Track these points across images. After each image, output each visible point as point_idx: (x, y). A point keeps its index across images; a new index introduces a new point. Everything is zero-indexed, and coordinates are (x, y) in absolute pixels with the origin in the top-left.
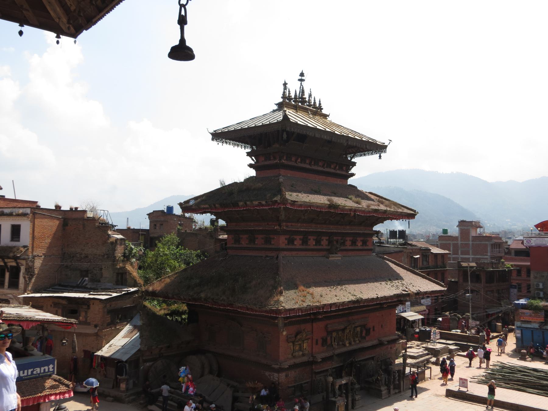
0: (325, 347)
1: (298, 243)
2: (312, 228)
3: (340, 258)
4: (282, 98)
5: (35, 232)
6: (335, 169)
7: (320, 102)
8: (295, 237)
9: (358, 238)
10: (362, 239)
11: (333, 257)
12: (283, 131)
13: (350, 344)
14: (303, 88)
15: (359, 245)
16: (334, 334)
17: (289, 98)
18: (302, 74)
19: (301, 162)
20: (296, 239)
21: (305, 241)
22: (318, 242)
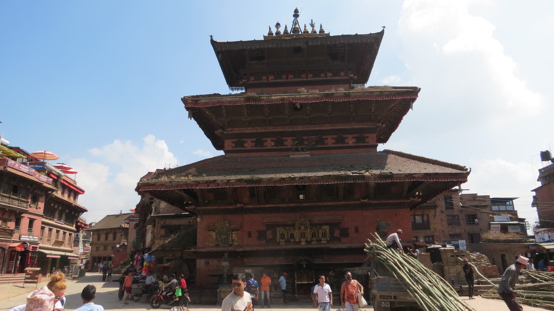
1: (249, 144)
2: (271, 129)
3: (309, 156)
4: (269, 34)
7: (321, 26)
8: (245, 140)
10: (355, 135)
11: (294, 155)
13: (308, 242)
15: (350, 142)
16: (279, 230)
17: (278, 33)
18: (296, 11)
19: (274, 79)
20: (246, 142)
22: (279, 142)
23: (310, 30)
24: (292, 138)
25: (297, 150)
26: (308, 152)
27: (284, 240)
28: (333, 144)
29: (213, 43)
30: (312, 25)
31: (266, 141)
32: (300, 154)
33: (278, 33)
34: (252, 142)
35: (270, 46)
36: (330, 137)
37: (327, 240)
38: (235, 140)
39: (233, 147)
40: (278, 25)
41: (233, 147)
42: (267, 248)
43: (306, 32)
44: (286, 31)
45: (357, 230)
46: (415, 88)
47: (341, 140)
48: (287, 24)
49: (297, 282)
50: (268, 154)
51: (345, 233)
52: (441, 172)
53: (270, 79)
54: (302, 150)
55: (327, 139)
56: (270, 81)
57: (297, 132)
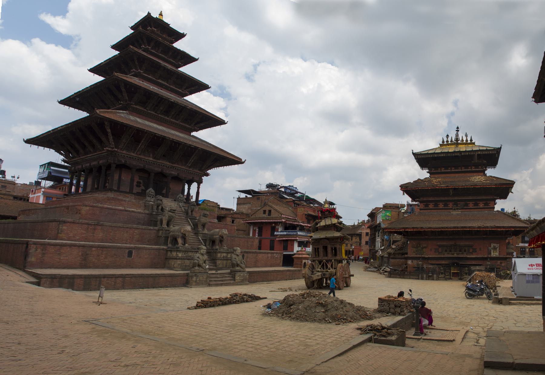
17: (447, 141)
18: (458, 128)
21: (436, 205)
22: (446, 205)
23: (465, 139)
25: (455, 210)
29: (414, 154)
30: (466, 136)
33: (447, 141)
36: (471, 203)
40: (448, 136)
43: (462, 140)
44: (451, 141)
47: (476, 204)
49: (452, 272)
50: (440, 211)
51: (475, 251)
54: (457, 209)
56: (443, 171)
57: (455, 200)
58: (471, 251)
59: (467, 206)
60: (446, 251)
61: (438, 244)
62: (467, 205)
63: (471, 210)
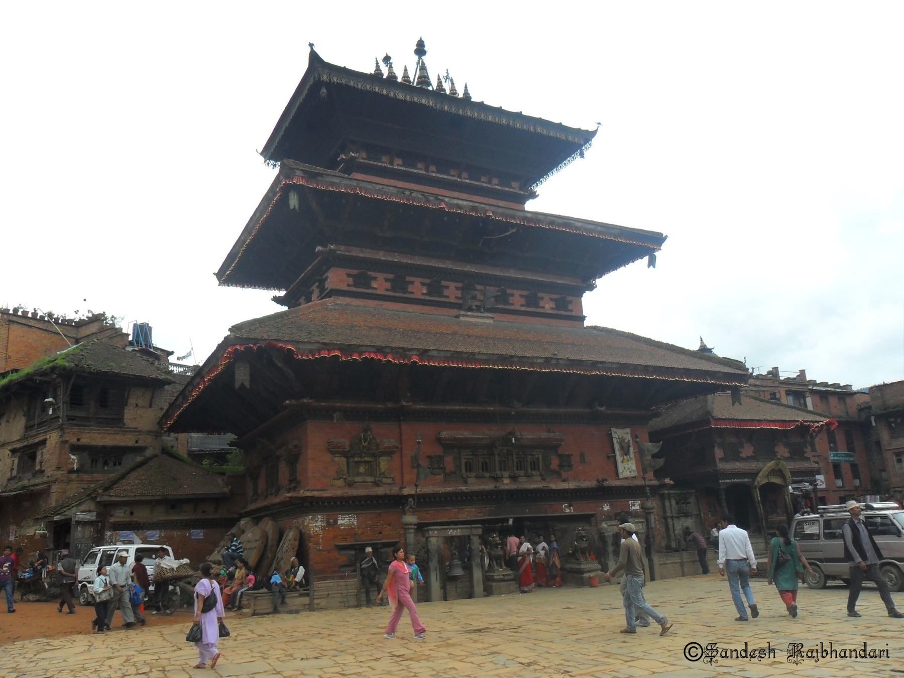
0: (440, 477)
1: (380, 284)
3: (491, 321)
5: (9, 350)
6: (490, 182)
8: (373, 274)
9: (540, 295)
11: (468, 316)
12: (318, 84)
13: (514, 478)
14: (423, 63)
15: (547, 306)
20: (375, 278)
21: (399, 285)
22: (435, 289)
23: (447, 87)
24: (460, 285)
25: (470, 309)
26: (486, 314)
27: (473, 474)
28: (522, 306)
31: (412, 283)
32: (477, 317)
34: (387, 280)
35: (423, 101)
36: (517, 293)
37: (541, 475)
38: (355, 272)
39: (349, 285)
40: (387, 59)
41: (349, 285)
42: (449, 489)
45: (583, 460)
46: (660, 234)
48: (404, 65)
51: (566, 462)
52: (717, 369)
53: (395, 164)
54: (478, 309)
55: (512, 295)
56: (396, 167)
57: (465, 275)
58: (555, 463)
59: (506, 302)
60: (469, 468)
61: (444, 434)
62: (503, 298)
63: (522, 319)
